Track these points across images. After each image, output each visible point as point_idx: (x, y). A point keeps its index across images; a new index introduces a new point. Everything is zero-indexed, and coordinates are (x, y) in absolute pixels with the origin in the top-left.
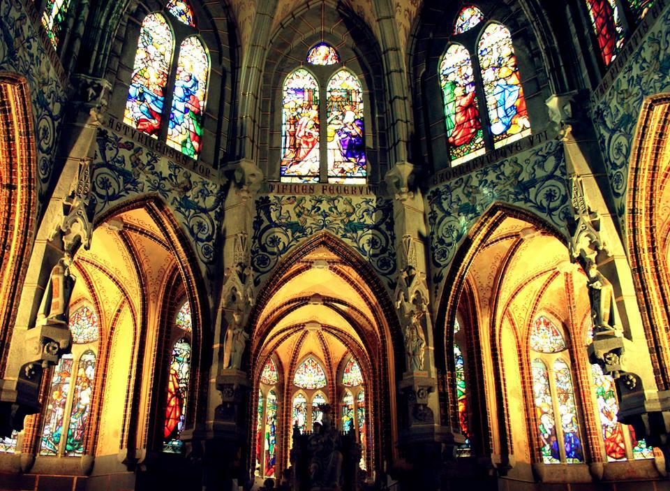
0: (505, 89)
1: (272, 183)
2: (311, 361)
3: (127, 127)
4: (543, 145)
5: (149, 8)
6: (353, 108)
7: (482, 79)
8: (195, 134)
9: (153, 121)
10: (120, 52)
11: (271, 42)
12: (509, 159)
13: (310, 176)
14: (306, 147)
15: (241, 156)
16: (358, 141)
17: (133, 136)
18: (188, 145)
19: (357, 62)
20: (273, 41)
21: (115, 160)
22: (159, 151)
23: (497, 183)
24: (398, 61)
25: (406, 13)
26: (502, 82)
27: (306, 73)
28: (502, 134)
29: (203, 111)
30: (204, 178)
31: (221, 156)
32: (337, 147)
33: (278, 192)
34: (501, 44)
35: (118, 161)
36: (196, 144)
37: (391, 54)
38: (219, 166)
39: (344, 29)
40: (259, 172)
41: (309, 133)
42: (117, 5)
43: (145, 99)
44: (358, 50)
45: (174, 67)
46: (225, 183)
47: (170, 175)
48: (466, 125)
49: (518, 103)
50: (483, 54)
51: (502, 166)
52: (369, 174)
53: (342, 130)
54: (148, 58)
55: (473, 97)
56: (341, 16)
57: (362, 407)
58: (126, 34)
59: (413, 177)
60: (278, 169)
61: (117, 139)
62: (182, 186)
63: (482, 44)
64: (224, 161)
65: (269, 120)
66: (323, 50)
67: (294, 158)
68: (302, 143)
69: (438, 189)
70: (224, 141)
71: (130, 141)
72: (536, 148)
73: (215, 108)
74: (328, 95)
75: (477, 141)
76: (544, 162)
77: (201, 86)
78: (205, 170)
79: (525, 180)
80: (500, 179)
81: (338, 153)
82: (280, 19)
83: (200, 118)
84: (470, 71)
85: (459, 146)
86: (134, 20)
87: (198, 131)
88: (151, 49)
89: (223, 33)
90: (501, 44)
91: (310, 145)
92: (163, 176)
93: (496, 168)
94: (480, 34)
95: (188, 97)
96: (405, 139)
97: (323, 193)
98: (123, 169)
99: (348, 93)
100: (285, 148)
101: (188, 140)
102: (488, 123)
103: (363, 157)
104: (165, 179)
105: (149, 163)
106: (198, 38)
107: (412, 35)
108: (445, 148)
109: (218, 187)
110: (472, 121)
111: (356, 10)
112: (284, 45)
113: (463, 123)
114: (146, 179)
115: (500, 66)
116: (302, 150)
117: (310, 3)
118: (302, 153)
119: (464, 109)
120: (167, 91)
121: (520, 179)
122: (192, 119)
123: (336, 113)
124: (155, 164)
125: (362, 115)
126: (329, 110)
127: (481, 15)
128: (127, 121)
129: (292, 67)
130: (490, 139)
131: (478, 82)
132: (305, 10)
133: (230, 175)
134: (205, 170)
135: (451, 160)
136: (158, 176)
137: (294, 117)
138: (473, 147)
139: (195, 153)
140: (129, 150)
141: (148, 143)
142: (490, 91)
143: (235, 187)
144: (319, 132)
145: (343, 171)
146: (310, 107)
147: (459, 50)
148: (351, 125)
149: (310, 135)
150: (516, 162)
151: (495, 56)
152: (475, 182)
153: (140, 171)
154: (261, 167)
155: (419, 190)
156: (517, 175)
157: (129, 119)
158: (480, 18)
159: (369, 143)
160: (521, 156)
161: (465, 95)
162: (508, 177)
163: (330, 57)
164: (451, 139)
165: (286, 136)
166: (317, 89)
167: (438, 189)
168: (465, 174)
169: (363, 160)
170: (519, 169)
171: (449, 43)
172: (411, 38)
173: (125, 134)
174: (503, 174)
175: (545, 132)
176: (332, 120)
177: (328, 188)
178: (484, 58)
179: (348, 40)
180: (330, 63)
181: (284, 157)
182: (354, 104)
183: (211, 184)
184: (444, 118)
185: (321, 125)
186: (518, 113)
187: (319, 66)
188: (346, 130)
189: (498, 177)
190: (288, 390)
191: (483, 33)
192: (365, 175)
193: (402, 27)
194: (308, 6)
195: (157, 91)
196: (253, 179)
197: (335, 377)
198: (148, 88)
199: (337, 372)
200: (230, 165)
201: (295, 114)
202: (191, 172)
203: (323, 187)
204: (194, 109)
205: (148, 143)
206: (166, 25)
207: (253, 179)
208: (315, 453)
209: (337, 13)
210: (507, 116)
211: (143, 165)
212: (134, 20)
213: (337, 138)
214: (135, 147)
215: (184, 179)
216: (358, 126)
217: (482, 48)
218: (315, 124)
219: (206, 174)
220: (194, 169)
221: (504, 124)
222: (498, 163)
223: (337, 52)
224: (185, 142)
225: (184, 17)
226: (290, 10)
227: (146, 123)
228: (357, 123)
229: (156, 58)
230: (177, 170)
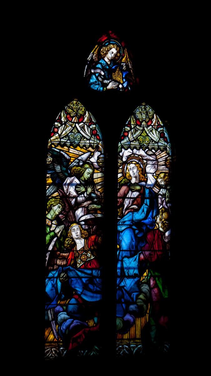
77: (162, 204)
95: (144, 237)
227: (81, 332)
229: (80, 199)
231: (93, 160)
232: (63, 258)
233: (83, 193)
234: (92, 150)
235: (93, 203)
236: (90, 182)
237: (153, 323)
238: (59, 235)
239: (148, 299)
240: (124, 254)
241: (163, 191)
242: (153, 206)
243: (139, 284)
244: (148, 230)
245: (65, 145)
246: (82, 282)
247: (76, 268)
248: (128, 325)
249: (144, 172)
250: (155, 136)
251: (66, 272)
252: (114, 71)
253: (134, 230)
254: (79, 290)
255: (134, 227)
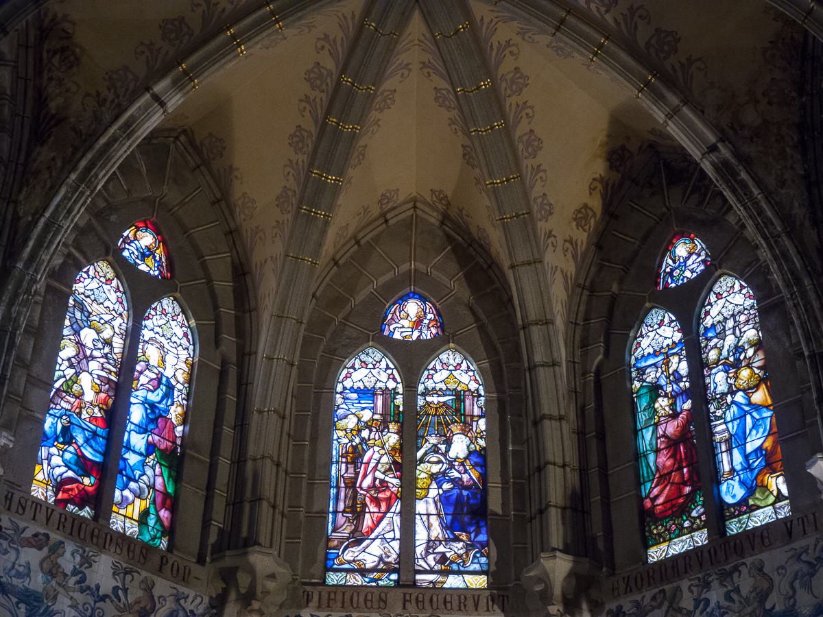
0: (746, 413)
1: (308, 588)
3: (37, 504)
4: (809, 541)
5: (86, 257)
6: (466, 429)
7: (706, 387)
8: (165, 494)
9: (86, 481)
10: (29, 357)
11: (314, 296)
12: (748, 561)
13: (382, 571)
14: (376, 510)
15: (250, 542)
16: (475, 495)
17: (48, 520)
18: (152, 521)
19: (476, 332)
20: (318, 294)
21: (13, 572)
22: (97, 544)
23: (728, 608)
24: (549, 343)
25: (568, 245)
26: (739, 398)
27: (378, 356)
28: (739, 504)
29: (181, 446)
30: (178, 587)
31: (213, 538)
32: (432, 510)
33: (319, 607)
34: (743, 318)
35: (19, 575)
36: (164, 514)
37: (536, 333)
38: (208, 559)
39: (453, 266)
40: (283, 571)
41: (382, 481)
42: (28, 278)
43: (73, 437)
44: (479, 311)
45: (127, 366)
46: (220, 591)
47: (116, 589)
48: (675, 477)
49: (768, 444)
50: (710, 335)
51: (736, 575)
52: (493, 568)
53: (444, 473)
54: (81, 356)
55: (688, 422)
56: (449, 238)
58: (41, 319)
59: (574, 581)
60: (321, 557)
61: (17, 530)
62: (137, 608)
63: (707, 313)
64: (218, 550)
65: (306, 457)
66: (412, 307)
67: (352, 532)
68: (367, 500)
69: (620, 608)
70: (219, 506)
71: (42, 531)
72: (799, 544)
73: (205, 438)
74: (421, 402)
75: (694, 514)
76: (812, 575)
78: (181, 571)
79: (777, 609)
80: (732, 600)
81: (434, 520)
82: (331, 251)
83: (174, 460)
84: (684, 368)
85: (662, 520)
86: (57, 285)
87: (170, 490)
88: (88, 336)
89: (224, 286)
90: (743, 318)
91: (383, 508)
92: (101, 593)
93: (725, 576)
94: (703, 294)
95: (156, 419)
96: (560, 502)
97: (404, 608)
98: (27, 589)
99: (459, 396)
100: (335, 512)
101: (152, 510)
102: (715, 478)
103: (484, 530)
104: (103, 598)
105: (75, 572)
106: (175, 299)
107: (579, 286)
108: (636, 521)
109: (206, 600)
110: (685, 470)
111: (474, 230)
112: (337, 302)
113: (669, 474)
114: (70, 603)
115: (737, 365)
116: (367, 516)
117: (389, 216)
118: (368, 521)
119: (672, 443)
120: (114, 417)
121: (768, 606)
122: (161, 465)
123: (433, 440)
124: (87, 572)
125: (482, 442)
126: (420, 433)
127: (707, 255)
128: (39, 491)
129: (353, 346)
130: (719, 513)
131: (699, 391)
132: (381, 228)
133: (228, 576)
134: (181, 571)
135: (647, 547)
136: (93, 595)
137: (355, 448)
138: (687, 524)
139: (163, 535)
140: (40, 549)
141: (76, 529)
142: (719, 413)
143: (237, 600)
144: (400, 478)
145: (443, 559)
146: (383, 425)
147: (666, 320)
148: (462, 464)
149: (384, 485)
150: (761, 570)
151: (730, 340)
152: (687, 602)
153: (61, 590)
154: (288, 558)
155: (584, 606)
156: (763, 597)
157: (39, 491)
158: (704, 262)
159: (495, 503)
160: (773, 558)
161: (675, 415)
162: (747, 599)
163: (426, 321)
164: (648, 503)
165: (338, 487)
166: (400, 390)
167: (620, 608)
168: (669, 582)
169: (483, 537)
170: (766, 585)
171: (647, 305)
172: (578, 290)
173: (34, 519)
174: (737, 590)
175: (814, 514)
176: (426, 454)
177: (413, 597)
178: (712, 343)
179: (458, 288)
180: (427, 335)
181: (334, 531)
182: (468, 419)
183: (190, 599)
184: (638, 456)
185: (404, 463)
186: (770, 467)
187: (403, 343)
188: (455, 474)
189: (728, 597)
191: (709, 294)
192: (485, 568)
193: (558, 275)
194: (386, 221)
195: (96, 418)
196: (271, 585)
198: (79, 414)
200: (229, 561)
201: (357, 440)
202: (155, 578)
203: (405, 594)
204: (164, 444)
205: (76, 529)
206: (115, 283)
207: (271, 585)
209: (439, 232)
210: (748, 467)
211: (65, 575)
212: (57, 285)
213: (434, 492)
214: (51, 543)
215: (140, 593)
216: (474, 466)
217: (708, 322)
218: (395, 462)
219: (183, 577)
220: (161, 569)
221: (742, 483)
222: (728, 567)
223: (439, 313)
224: (145, 514)
225: (149, 261)
226: (351, 231)
227: (74, 485)
228: (474, 459)
229: (96, 353)
230: (129, 577)
231: (116, 323)
232: (68, 402)
233: (100, 349)
234: (116, 315)
235: (109, 363)
236: (108, 342)
237: (152, 510)
238: (68, 378)
239: (151, 486)
240: (133, 427)
241: (179, 386)
242: (169, 392)
243: (144, 464)
244: (161, 416)
245: (88, 297)
246: (84, 434)
247: (80, 418)
248: (124, 502)
249: (163, 360)
250: (180, 332)
251: (69, 416)
252: (148, 256)
253: (146, 409)
254: (80, 440)
255: (146, 405)
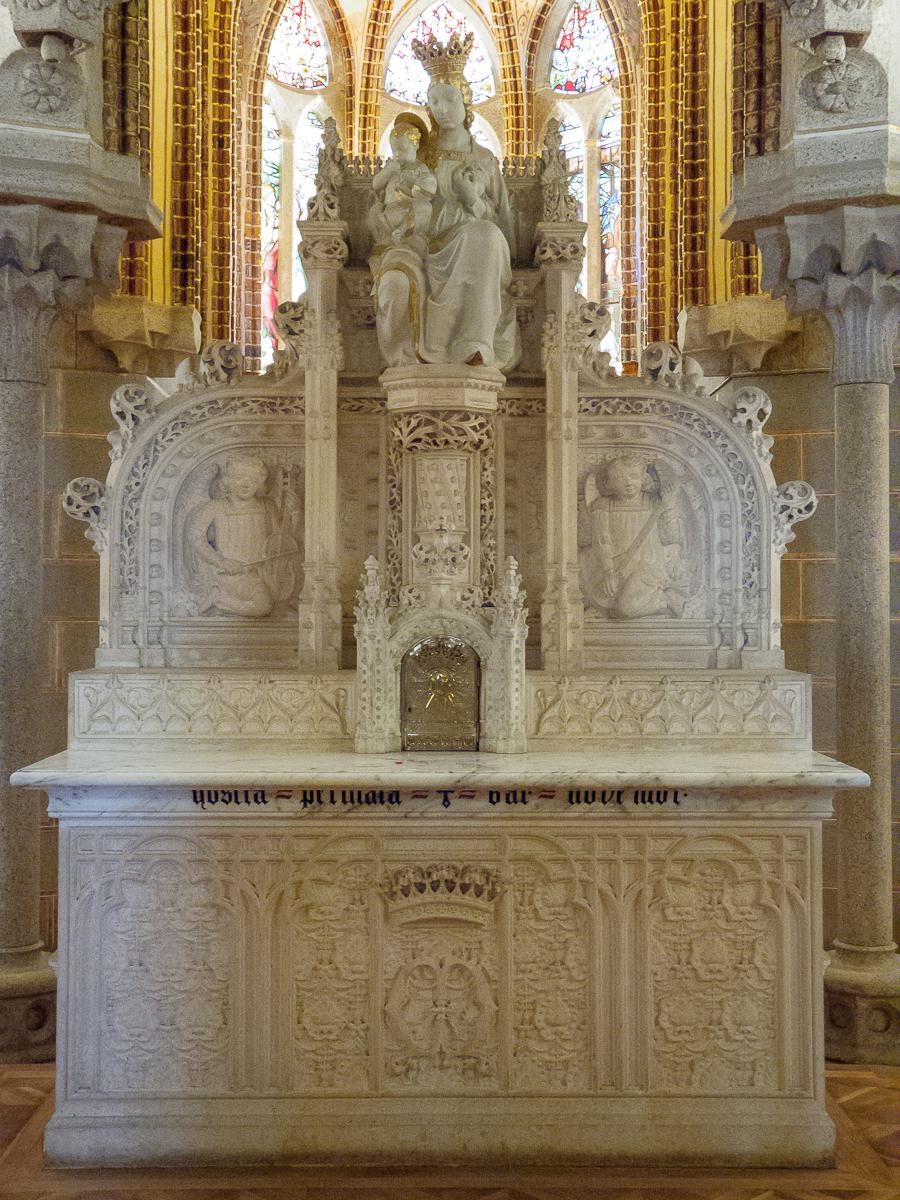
2: (442, 13)
57: (614, 164)
190: (365, 109)
197: (523, 64)
199: (532, 48)
208: (397, 234)
